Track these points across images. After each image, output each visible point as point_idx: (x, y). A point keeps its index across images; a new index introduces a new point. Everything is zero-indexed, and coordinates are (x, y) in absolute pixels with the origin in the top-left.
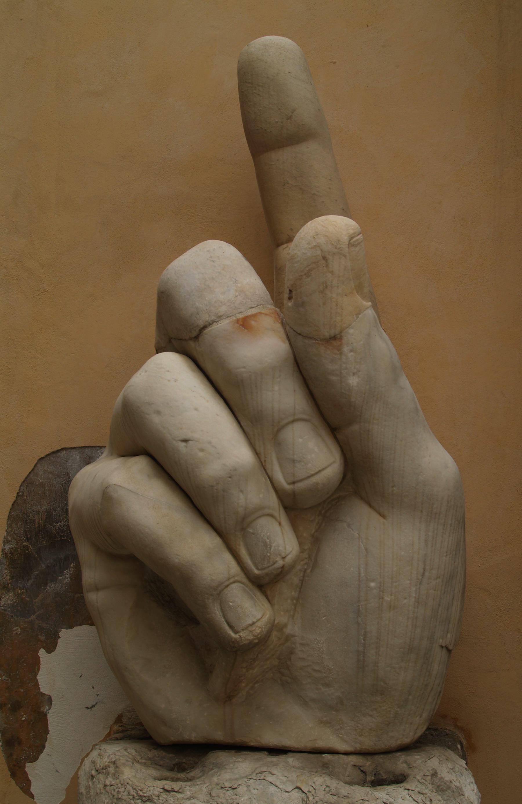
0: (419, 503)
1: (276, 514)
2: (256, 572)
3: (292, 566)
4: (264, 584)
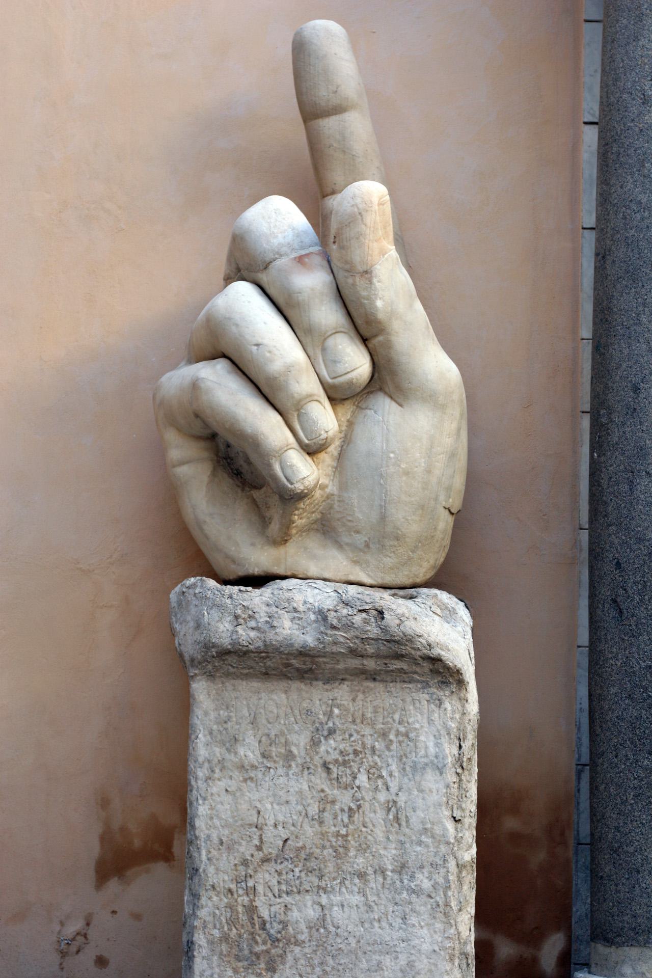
0: (430, 398)
1: (322, 401)
2: (307, 441)
3: (333, 439)
4: (312, 451)
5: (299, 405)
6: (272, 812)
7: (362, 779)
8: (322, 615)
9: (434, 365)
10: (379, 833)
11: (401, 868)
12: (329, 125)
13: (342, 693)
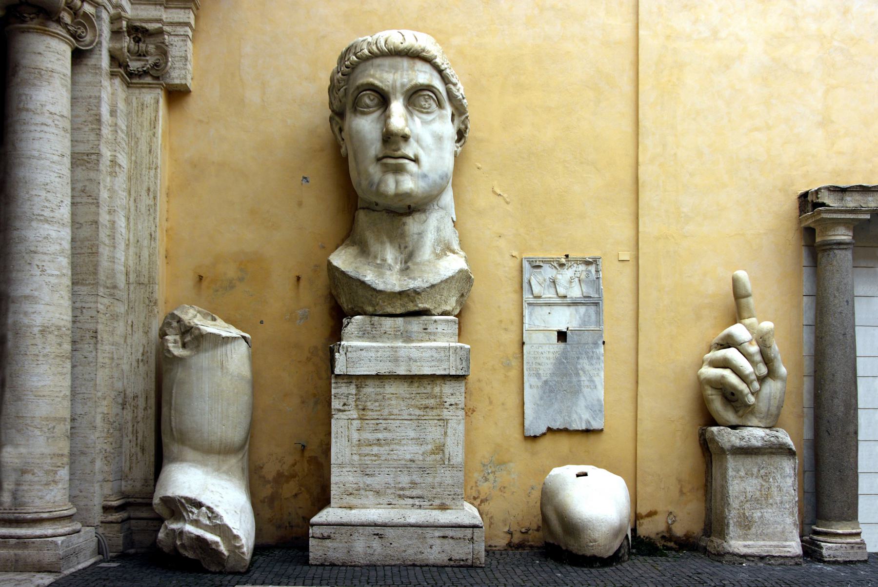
5: (752, 382)
6: (749, 489)
7: (771, 480)
8: (763, 438)
9: (783, 370)
10: (776, 494)
11: (781, 503)
12: (743, 301)
13: (765, 458)
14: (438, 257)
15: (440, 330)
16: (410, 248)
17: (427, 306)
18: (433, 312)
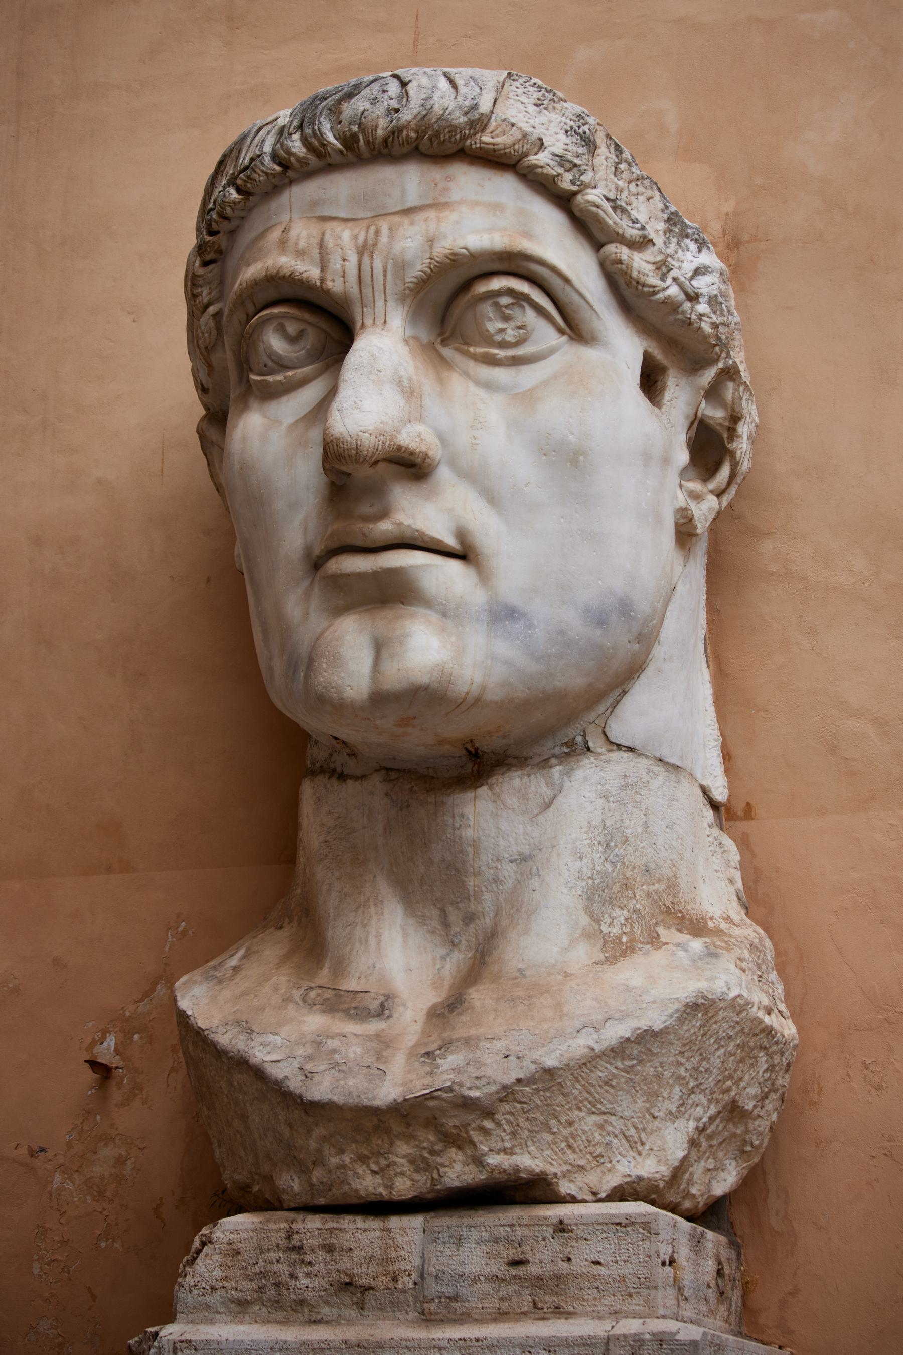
14: (617, 950)
15: (580, 1264)
16: (488, 921)
17: (529, 1161)
18: (565, 1188)
